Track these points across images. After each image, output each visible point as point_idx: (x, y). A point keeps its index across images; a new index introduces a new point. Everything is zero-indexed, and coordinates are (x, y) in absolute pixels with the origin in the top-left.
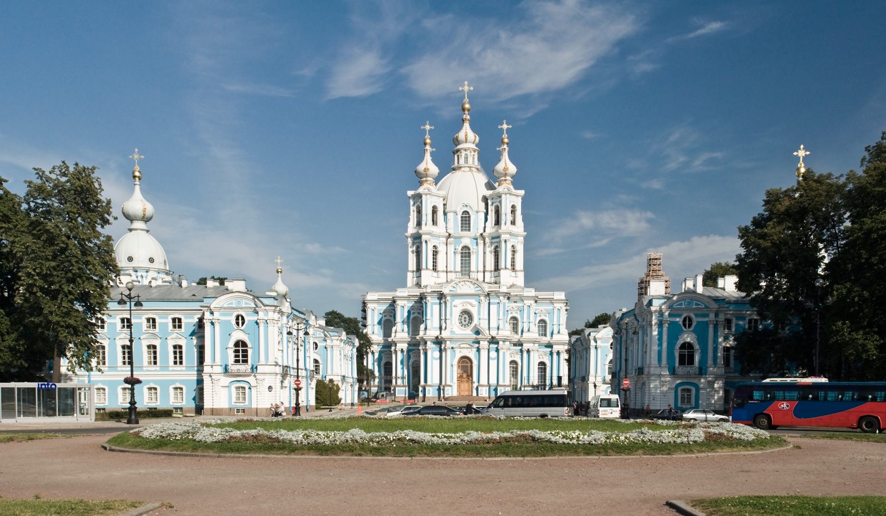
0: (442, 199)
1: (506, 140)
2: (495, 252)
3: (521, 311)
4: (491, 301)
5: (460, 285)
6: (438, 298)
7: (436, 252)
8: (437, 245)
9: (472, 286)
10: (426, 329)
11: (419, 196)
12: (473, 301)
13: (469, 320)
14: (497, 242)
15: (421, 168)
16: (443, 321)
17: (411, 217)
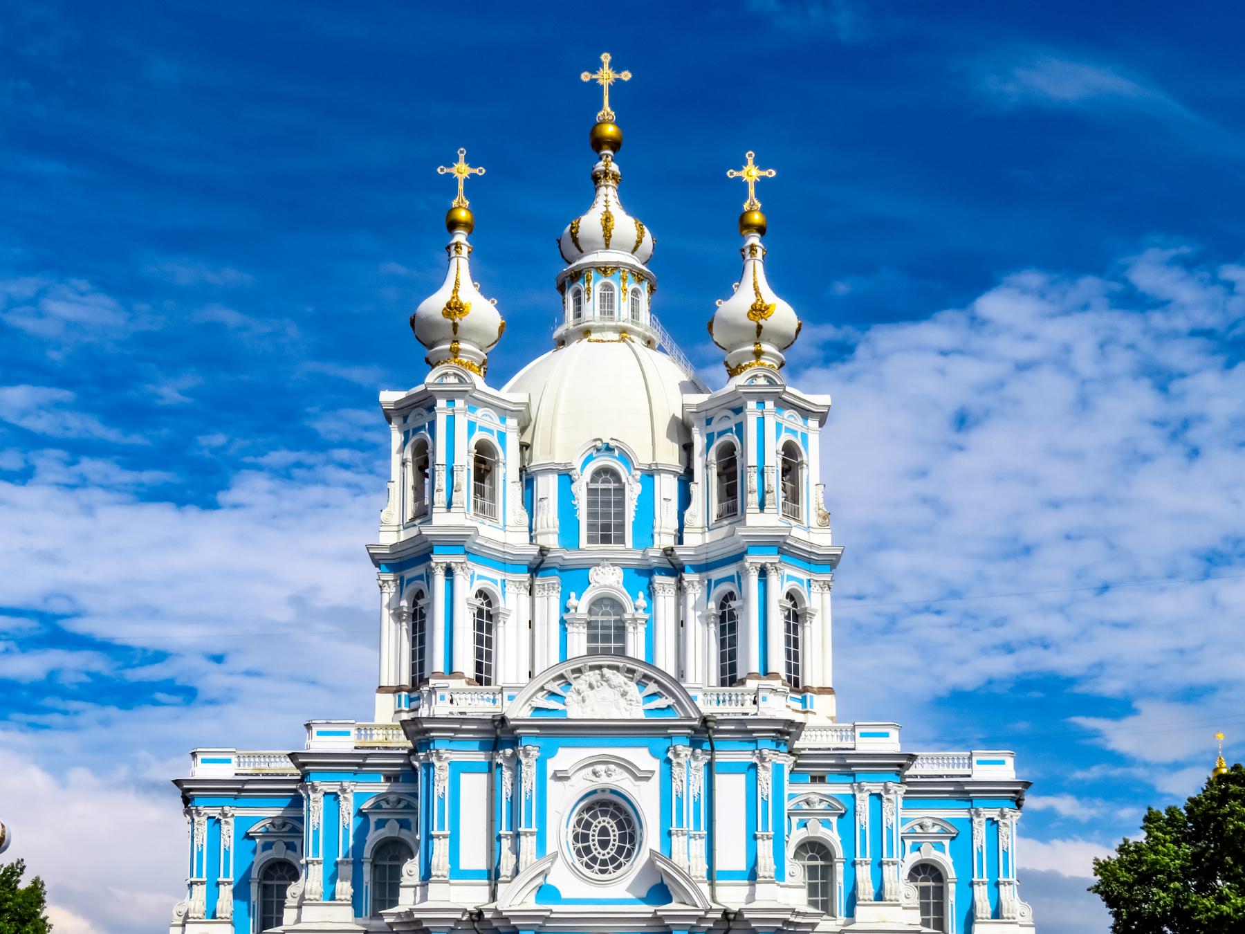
0: (512, 423)
1: (757, 218)
2: (722, 618)
3: (846, 815)
4: (720, 758)
5: (580, 683)
6: (484, 747)
7: (490, 617)
8: (497, 590)
9: (633, 688)
10: (427, 876)
11: (426, 403)
12: (641, 757)
13: (622, 838)
14: (730, 579)
15: (433, 305)
16: (506, 844)
17: (395, 488)
